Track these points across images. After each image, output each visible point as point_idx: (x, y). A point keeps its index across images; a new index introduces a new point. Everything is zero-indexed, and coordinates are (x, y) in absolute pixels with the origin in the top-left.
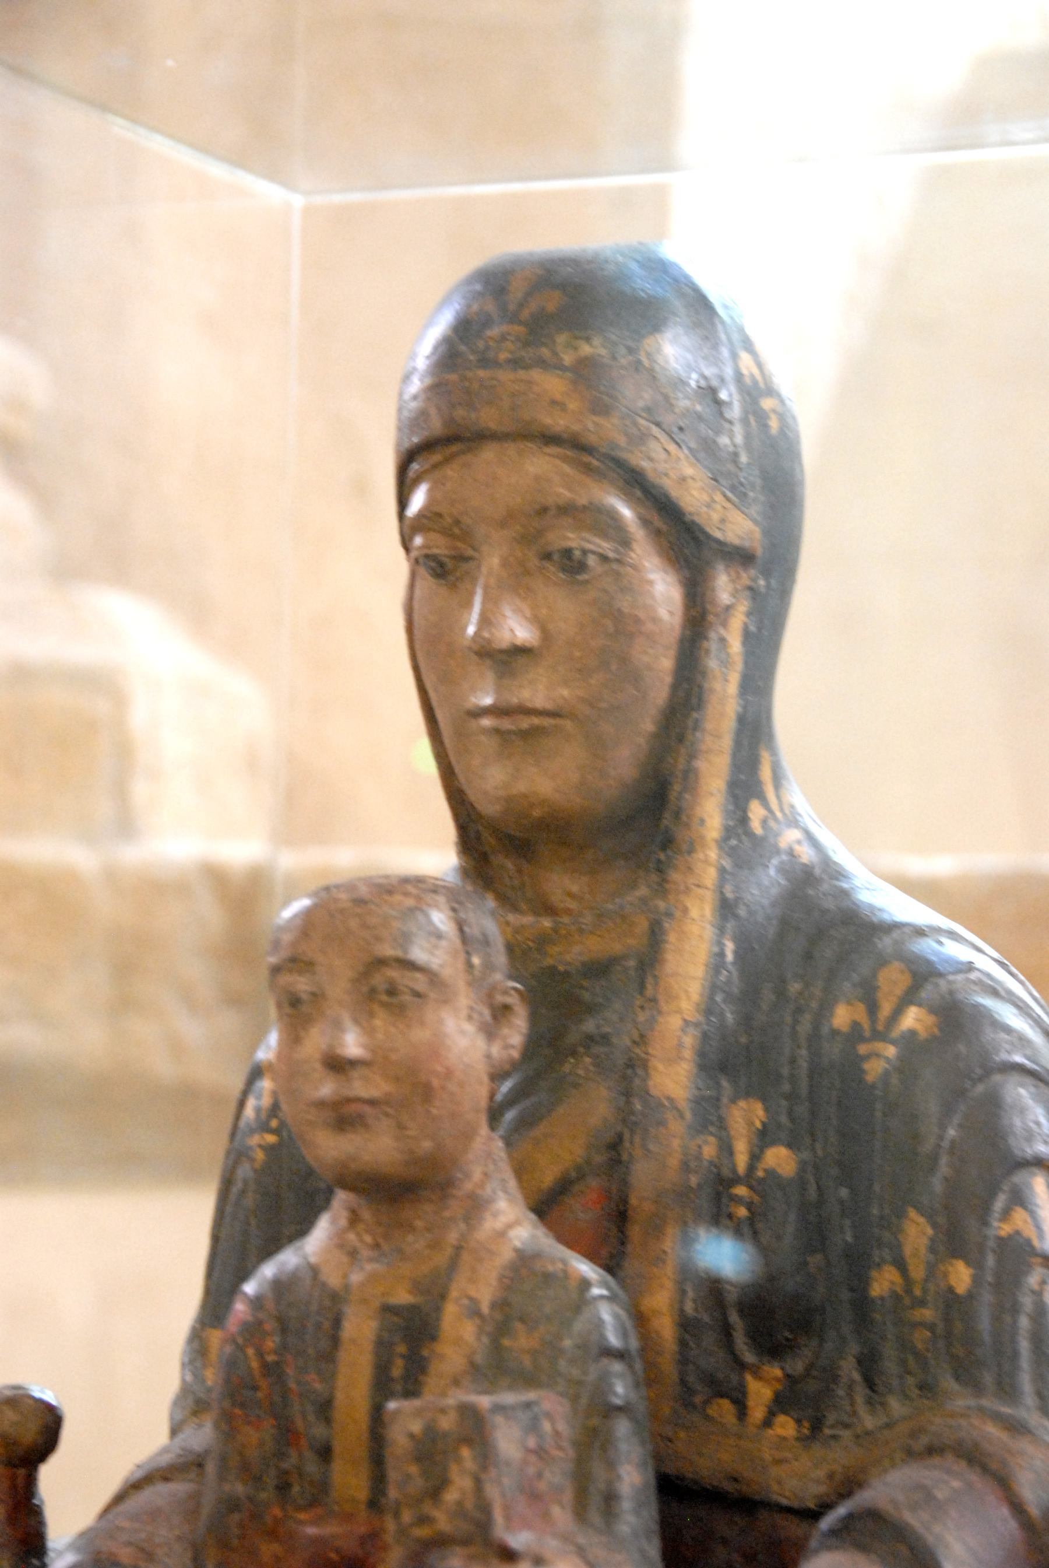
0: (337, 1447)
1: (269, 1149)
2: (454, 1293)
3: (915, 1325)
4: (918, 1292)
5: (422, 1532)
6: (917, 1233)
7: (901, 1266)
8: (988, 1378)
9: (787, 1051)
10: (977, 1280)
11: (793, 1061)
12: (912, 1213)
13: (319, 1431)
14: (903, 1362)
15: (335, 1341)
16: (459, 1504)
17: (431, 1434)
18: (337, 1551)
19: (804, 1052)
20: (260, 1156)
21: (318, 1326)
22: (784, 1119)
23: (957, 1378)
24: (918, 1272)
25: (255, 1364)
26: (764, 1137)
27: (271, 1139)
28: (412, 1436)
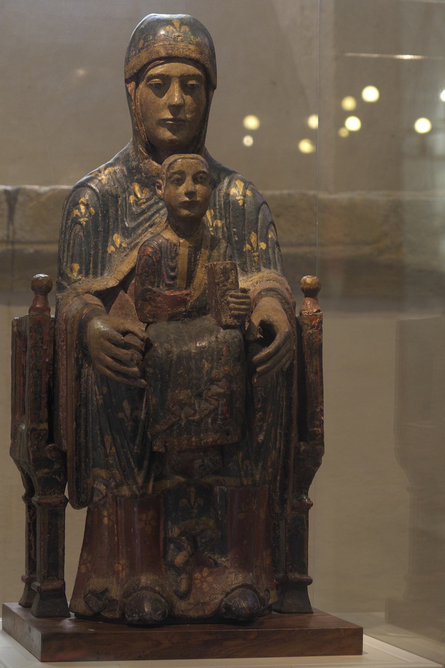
0: (179, 276)
1: (86, 221)
2: (203, 244)
3: (254, 256)
4: (255, 250)
5: (225, 288)
6: (253, 238)
7: (251, 245)
8: (272, 267)
9: (217, 199)
10: (267, 246)
11: (219, 201)
12: (253, 233)
13: (172, 274)
14: (251, 265)
15: (177, 254)
16: (232, 282)
17: (225, 268)
18: (179, 298)
19: (222, 199)
20: (84, 223)
21: (171, 252)
22: (218, 214)
23: (264, 267)
24: (254, 245)
25: (155, 260)
26: (214, 217)
27: (86, 219)
28: (221, 269)
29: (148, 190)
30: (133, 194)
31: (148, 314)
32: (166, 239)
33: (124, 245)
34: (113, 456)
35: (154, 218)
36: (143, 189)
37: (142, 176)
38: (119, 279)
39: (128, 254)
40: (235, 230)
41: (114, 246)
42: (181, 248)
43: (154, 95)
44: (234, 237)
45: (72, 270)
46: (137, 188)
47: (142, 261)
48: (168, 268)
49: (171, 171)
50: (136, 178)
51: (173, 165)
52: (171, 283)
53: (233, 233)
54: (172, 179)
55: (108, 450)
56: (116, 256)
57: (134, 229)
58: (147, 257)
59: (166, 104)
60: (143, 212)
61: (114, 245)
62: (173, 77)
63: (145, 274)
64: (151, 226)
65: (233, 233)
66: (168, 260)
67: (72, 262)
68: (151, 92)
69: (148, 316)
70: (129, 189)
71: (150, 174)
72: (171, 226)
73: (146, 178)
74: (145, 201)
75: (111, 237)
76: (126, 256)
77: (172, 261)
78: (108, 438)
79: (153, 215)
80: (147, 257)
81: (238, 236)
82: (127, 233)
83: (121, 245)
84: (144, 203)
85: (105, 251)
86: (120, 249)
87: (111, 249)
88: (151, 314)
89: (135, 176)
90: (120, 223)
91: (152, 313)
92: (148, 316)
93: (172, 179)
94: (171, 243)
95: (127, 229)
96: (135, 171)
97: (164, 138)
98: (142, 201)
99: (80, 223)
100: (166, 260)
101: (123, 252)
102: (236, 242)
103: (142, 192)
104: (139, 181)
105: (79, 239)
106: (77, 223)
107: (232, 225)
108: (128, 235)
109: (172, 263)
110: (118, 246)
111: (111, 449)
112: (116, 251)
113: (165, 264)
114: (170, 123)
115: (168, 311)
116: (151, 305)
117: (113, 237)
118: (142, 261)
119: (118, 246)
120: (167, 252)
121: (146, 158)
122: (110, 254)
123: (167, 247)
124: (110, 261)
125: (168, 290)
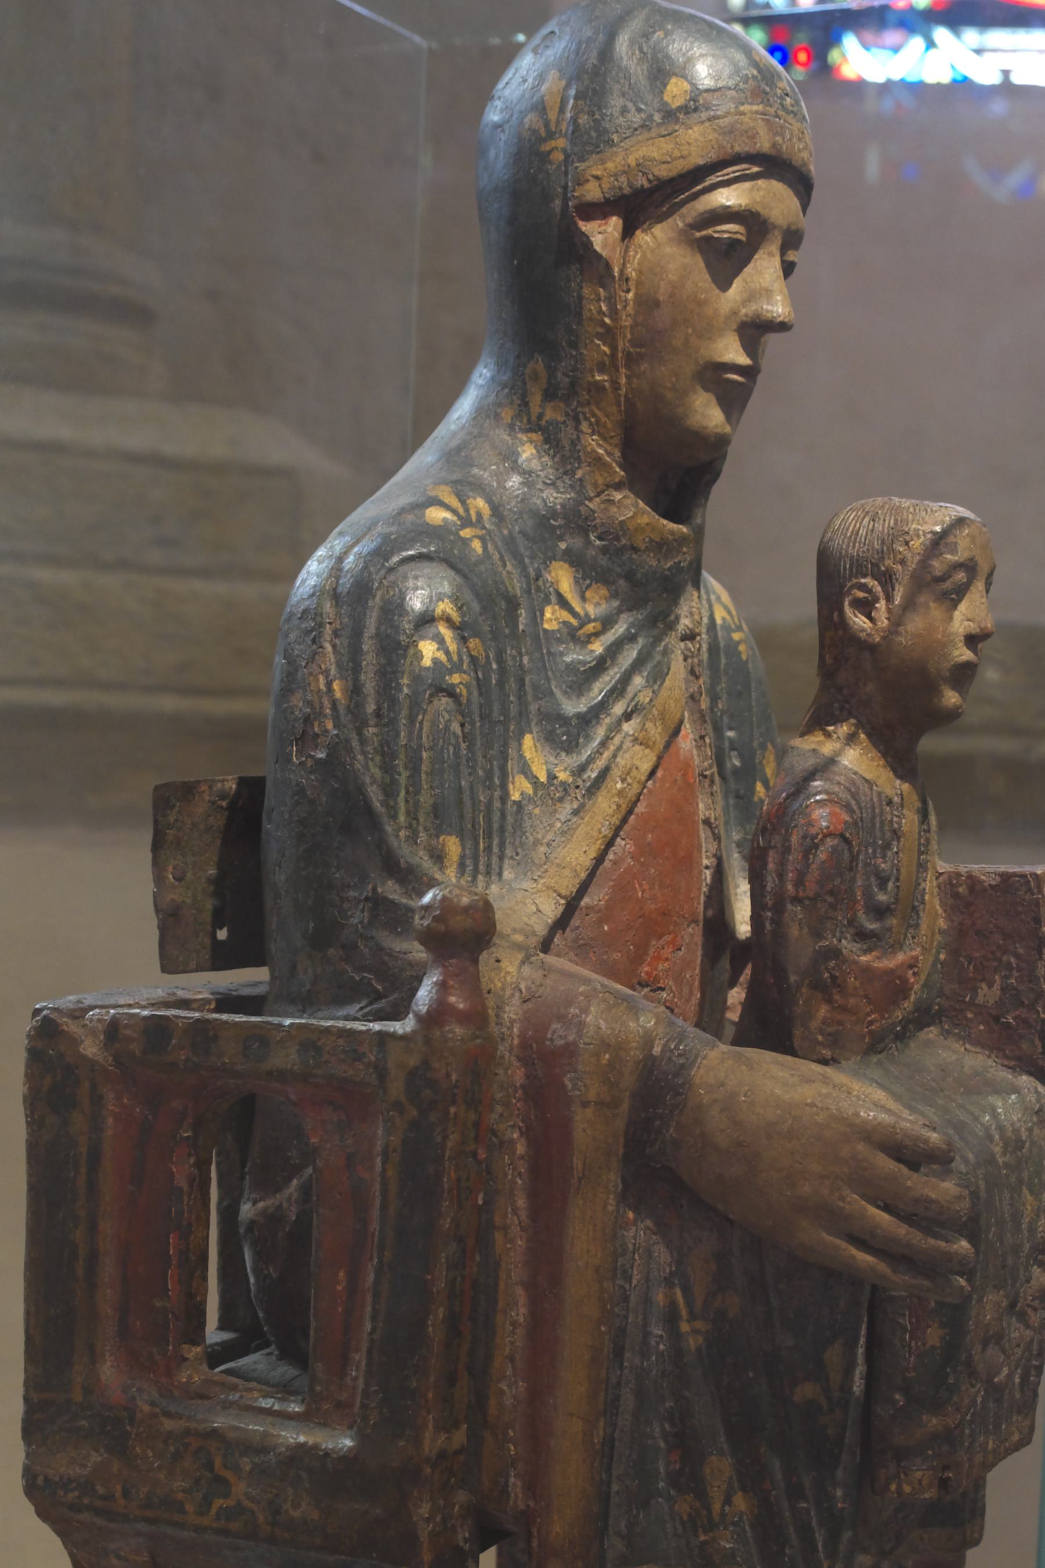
29: (604, 591)
30: (553, 598)
31: (821, 1032)
32: (867, 781)
33: (562, 776)
34: (733, 1523)
35: (631, 690)
36: (588, 587)
37: (588, 542)
38: (564, 892)
39: (582, 806)
40: (730, 734)
41: (527, 777)
42: (904, 811)
43: (707, 277)
44: (730, 758)
45: (439, 857)
46: (563, 578)
47: (822, 855)
48: (873, 879)
49: (949, 556)
50: (563, 546)
51: (951, 539)
52: (872, 926)
53: (727, 744)
54: (947, 585)
55: (717, 1507)
56: (537, 811)
57: (588, 719)
58: (836, 842)
59: (735, 313)
60: (601, 665)
61: (525, 770)
62: (774, 227)
63: (830, 899)
64: (627, 716)
65: (727, 744)
66: (874, 852)
67: (439, 831)
68: (702, 265)
69: (820, 1038)
70: (540, 583)
71: (624, 541)
72: (869, 735)
73: (604, 550)
74: (598, 625)
75: (513, 744)
76: (576, 813)
77: (884, 857)
78: (719, 1468)
79: (625, 680)
80: (836, 842)
81: (741, 756)
82: (565, 734)
83: (552, 777)
84: (597, 634)
85: (505, 797)
86: (550, 791)
87: (519, 788)
88: (830, 1034)
89: (561, 538)
90: (530, 698)
91: (830, 1030)
92: (820, 1038)
93: (947, 585)
94: (879, 794)
95: (564, 720)
96: (560, 522)
97: (706, 428)
98: (590, 627)
99: (450, 692)
100: (870, 851)
101: (561, 800)
102: (736, 771)
103: (583, 598)
104: (573, 559)
105: (451, 749)
106: (442, 690)
107: (726, 720)
108: (569, 741)
109: (885, 862)
110: (543, 778)
111: (728, 1501)
112: (535, 793)
113: (866, 865)
114: (735, 382)
115: (871, 1023)
116: (829, 1001)
117: (520, 745)
118: (822, 855)
119: (543, 778)
120: (874, 825)
121: (618, 486)
122: (518, 804)
123: (873, 808)
124: (518, 826)
125: (866, 952)
